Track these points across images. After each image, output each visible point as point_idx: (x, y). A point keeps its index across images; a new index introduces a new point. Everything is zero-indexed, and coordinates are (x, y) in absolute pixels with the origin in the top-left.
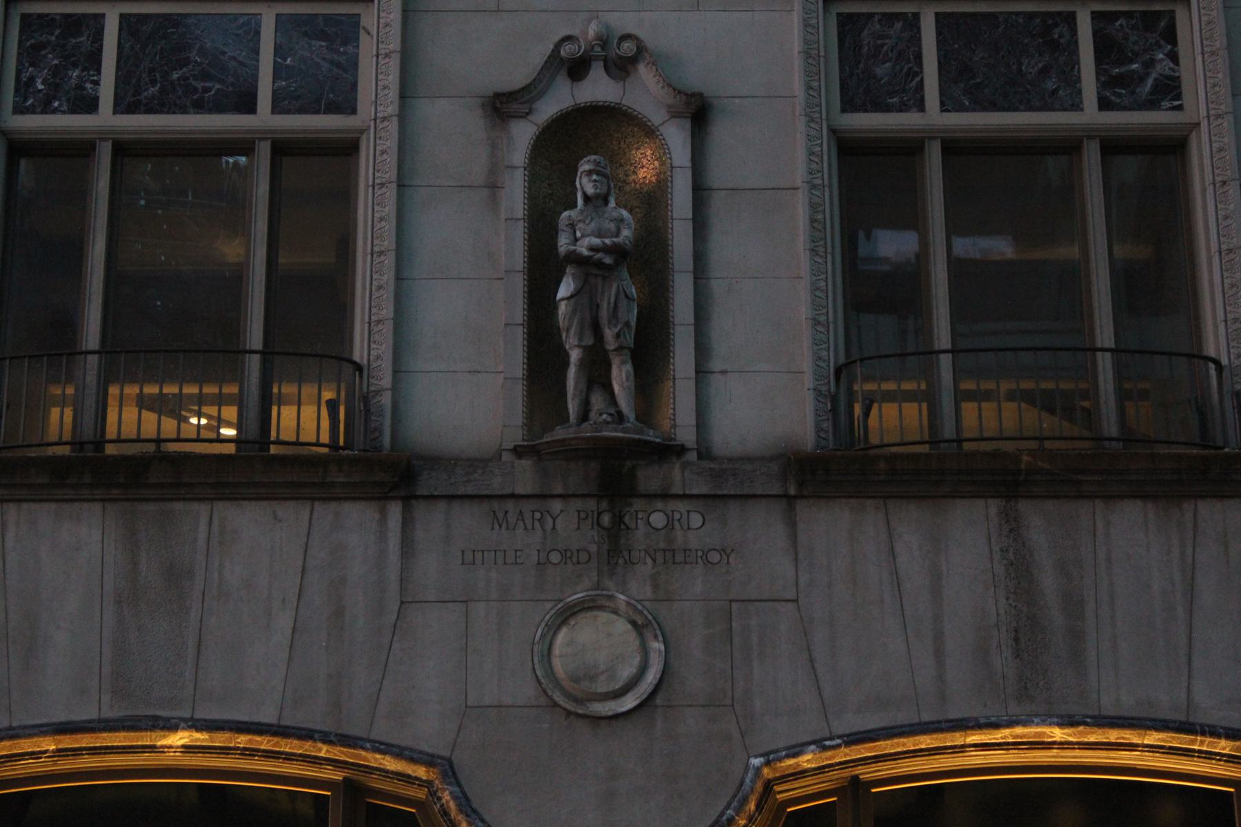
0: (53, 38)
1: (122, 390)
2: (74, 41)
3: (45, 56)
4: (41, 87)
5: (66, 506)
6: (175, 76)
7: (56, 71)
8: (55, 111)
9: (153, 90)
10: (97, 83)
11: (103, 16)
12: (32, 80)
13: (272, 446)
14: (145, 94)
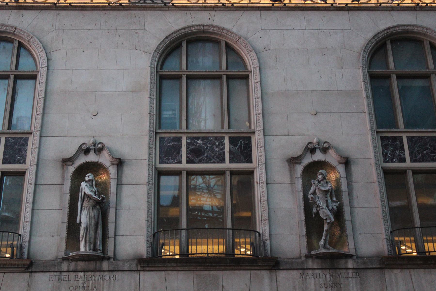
0: (390, 142)
1: (197, 240)
2: (396, 143)
3: (389, 147)
4: (389, 155)
5: (426, 270)
6: (425, 152)
7: (393, 151)
8: (394, 162)
9: (420, 156)
10: (404, 154)
11: (182, 137)
12: (386, 154)
13: (189, 255)
14: (418, 157)
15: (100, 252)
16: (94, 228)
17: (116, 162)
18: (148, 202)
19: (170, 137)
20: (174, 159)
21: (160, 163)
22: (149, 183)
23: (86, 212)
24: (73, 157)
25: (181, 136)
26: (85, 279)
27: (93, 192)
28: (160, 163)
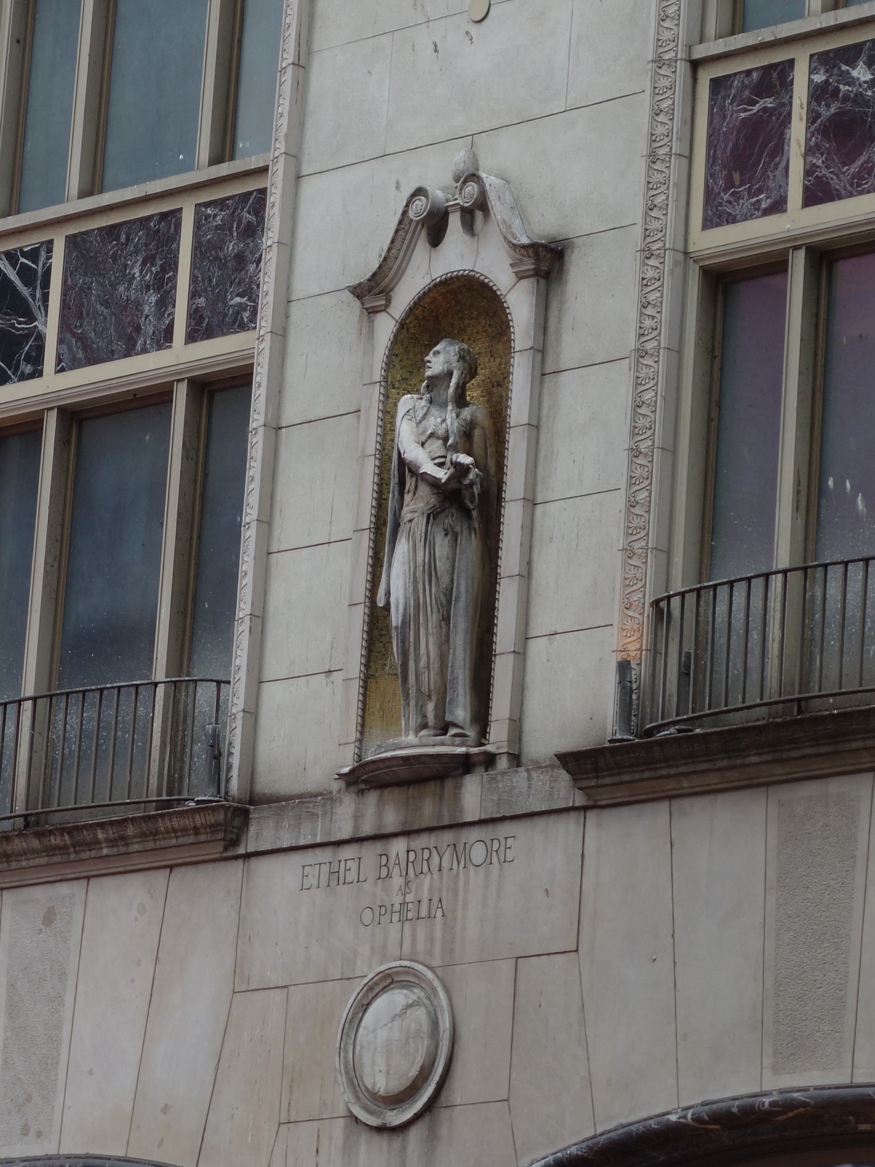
15: (455, 735)
16: (434, 619)
17: (529, 265)
18: (635, 452)
19: (748, 73)
20: (760, 191)
21: (708, 223)
22: (642, 353)
23: (406, 547)
24: (384, 269)
25: (790, 57)
26: (411, 870)
27: (438, 438)
28: (708, 223)
